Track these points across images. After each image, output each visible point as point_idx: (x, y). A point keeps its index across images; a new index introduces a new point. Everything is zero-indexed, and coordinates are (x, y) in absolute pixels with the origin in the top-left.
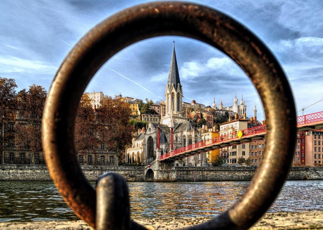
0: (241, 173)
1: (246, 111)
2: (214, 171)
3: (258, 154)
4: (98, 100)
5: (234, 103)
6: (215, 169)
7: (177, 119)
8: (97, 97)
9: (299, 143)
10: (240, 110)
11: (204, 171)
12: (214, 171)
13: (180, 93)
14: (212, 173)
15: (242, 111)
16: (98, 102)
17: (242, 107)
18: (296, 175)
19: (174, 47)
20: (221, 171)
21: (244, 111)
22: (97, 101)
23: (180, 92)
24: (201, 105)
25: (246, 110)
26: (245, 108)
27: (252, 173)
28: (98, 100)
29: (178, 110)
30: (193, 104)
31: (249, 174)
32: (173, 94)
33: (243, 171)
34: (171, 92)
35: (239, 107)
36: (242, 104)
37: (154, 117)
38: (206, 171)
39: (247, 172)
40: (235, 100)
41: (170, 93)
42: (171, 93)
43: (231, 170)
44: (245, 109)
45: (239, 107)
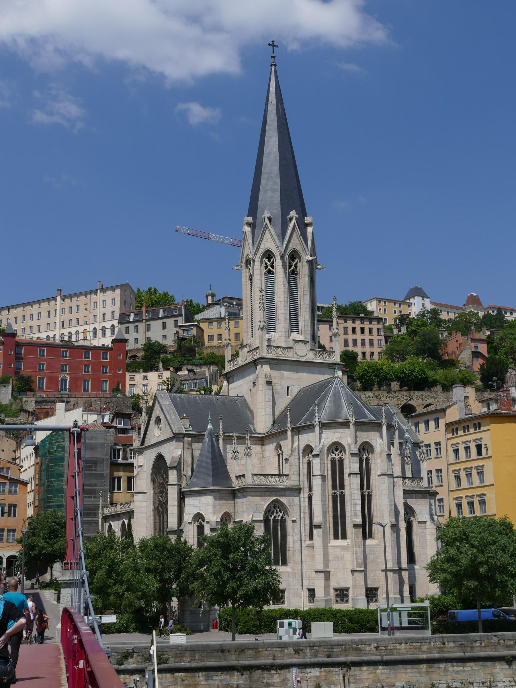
4: (113, 312)
8: (109, 302)
11: (359, 664)
13: (302, 253)
16: (113, 319)
22: (108, 316)
23: (299, 248)
28: (113, 312)
34: (258, 248)
41: (255, 254)
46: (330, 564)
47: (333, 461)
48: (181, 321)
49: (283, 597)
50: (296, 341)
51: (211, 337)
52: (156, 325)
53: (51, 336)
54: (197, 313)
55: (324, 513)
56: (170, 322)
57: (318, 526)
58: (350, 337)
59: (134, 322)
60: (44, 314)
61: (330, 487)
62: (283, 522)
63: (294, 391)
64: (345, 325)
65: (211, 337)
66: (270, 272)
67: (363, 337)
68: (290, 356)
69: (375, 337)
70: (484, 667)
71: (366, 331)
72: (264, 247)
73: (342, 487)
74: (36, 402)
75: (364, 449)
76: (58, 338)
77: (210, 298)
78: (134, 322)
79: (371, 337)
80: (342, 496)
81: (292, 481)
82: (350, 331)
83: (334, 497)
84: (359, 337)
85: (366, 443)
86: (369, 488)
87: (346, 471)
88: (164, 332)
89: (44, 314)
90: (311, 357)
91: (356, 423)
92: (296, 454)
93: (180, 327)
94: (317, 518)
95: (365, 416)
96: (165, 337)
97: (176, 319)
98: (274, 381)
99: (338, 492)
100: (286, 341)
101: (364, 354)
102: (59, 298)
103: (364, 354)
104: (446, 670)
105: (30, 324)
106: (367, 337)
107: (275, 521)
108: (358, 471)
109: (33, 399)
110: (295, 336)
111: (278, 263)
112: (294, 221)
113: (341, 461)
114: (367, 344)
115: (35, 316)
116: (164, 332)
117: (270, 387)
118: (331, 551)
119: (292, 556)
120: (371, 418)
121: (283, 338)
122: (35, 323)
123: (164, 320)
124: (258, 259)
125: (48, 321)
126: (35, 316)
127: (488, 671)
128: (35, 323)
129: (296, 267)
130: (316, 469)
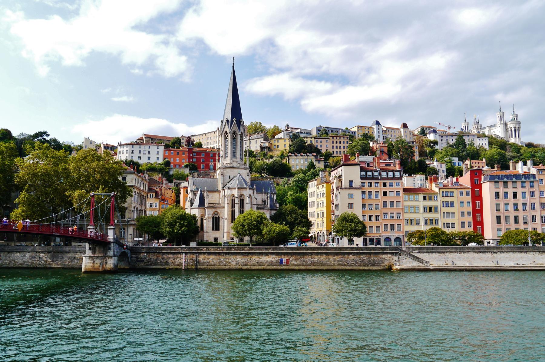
1: (521, 132)
3: (381, 218)
5: (498, 119)
7: (229, 170)
9: (469, 196)
10: (509, 129)
13: (237, 132)
14: (212, 257)
15: (513, 131)
17: (511, 126)
18: (370, 261)
20: (228, 253)
21: (517, 131)
23: (236, 130)
24: (425, 129)
25: (521, 129)
26: (517, 126)
29: (234, 155)
30: (402, 130)
31: (277, 259)
32: (227, 134)
34: (223, 130)
35: (506, 125)
36: (512, 120)
37: (306, 157)
39: (275, 256)
40: (498, 114)
41: (222, 132)
42: (224, 131)
44: (519, 127)
45: (506, 125)
47: (232, 200)
48: (262, 140)
49: (217, 240)
50: (233, 161)
53: (215, 146)
54: (276, 135)
55: (228, 215)
56: (258, 140)
58: (335, 145)
60: (212, 137)
61: (231, 208)
62: (219, 218)
63: (231, 177)
64: (333, 140)
66: (227, 138)
67: (340, 145)
68: (231, 165)
69: (346, 145)
71: (342, 142)
73: (234, 208)
74: (198, 174)
75: (242, 196)
76: (217, 147)
77: (287, 127)
79: (344, 145)
80: (234, 210)
81: (222, 205)
82: (335, 142)
83: (232, 210)
84: (338, 145)
85: (242, 194)
86: (243, 208)
87: (236, 203)
89: (212, 137)
90: (238, 166)
91: (238, 188)
92: (223, 197)
93: (262, 142)
94: (226, 217)
98: (225, 174)
99: (233, 209)
100: (230, 161)
101: (337, 152)
102: (218, 131)
103: (337, 152)
104: (223, 255)
105: (208, 141)
106: (342, 145)
107: (216, 217)
109: (196, 173)
110: (234, 159)
111: (229, 135)
113: (234, 200)
114: (338, 148)
115: (209, 138)
116: (256, 145)
117: (223, 176)
119: (221, 228)
120: (245, 186)
121: (229, 160)
122: (209, 141)
123: (256, 140)
124: (223, 134)
125: (214, 140)
126: (209, 138)
128: (209, 141)
129: (235, 136)
130: (226, 202)
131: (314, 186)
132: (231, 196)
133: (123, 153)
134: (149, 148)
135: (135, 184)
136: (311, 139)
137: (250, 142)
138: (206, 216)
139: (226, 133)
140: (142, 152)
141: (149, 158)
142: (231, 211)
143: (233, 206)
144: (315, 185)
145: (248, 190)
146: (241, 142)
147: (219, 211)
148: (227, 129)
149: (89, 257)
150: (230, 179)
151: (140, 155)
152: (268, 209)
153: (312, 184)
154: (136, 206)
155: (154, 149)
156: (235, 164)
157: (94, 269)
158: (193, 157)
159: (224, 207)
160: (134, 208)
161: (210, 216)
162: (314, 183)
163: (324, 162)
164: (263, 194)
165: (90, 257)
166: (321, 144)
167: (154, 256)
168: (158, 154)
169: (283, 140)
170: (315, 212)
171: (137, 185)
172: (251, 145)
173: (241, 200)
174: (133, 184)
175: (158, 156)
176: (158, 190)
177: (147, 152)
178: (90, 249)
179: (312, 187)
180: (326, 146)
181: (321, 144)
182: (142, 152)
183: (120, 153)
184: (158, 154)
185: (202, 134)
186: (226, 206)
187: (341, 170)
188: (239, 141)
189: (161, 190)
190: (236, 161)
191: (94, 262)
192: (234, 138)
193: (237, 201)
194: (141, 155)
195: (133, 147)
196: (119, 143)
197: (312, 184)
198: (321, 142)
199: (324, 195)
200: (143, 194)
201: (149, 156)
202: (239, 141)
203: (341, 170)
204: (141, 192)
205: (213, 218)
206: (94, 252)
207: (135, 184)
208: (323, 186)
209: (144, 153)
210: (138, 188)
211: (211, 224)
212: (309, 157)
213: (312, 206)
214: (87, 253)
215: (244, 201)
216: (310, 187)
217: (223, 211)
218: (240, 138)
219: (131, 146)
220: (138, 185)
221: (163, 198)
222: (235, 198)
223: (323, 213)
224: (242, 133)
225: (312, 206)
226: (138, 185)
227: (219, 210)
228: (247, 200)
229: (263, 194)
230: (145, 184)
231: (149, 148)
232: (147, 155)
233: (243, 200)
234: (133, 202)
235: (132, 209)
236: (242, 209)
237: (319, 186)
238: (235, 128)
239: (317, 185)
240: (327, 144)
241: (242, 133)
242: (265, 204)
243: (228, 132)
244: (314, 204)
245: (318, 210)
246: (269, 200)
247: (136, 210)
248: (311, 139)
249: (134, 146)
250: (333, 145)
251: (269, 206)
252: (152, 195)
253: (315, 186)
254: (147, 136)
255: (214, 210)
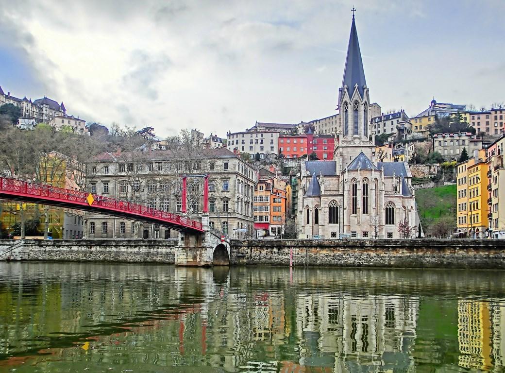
0: (389, 251)
2: (331, 247)
6: (333, 242)
7: (349, 150)
12: (331, 247)
13: (360, 101)
14: (324, 252)
19: (354, 16)
23: (358, 99)
27: (417, 253)
29: (356, 131)
32: (347, 104)
33: (394, 248)
37: (458, 138)
38: (314, 247)
39: (405, 251)
42: (343, 102)
43: (367, 247)
46: (351, 223)
47: (353, 185)
50: (355, 138)
51: (416, 127)
52: (388, 123)
55: (348, 204)
56: (395, 121)
57: (345, 209)
59: (378, 122)
61: (352, 195)
63: (353, 159)
64: (496, 115)
65: (416, 127)
66: (347, 111)
70: (352, 249)
72: (344, 100)
73: (356, 195)
78: (378, 122)
80: (356, 198)
82: (498, 118)
83: (353, 198)
88: (392, 126)
90: (362, 144)
92: (342, 182)
94: (346, 205)
95: (366, 167)
96: (392, 129)
97: (398, 119)
99: (355, 197)
105: (332, 127)
107: (334, 207)
108: (362, 189)
112: (356, 88)
113: (356, 185)
115: (334, 123)
116: (392, 126)
118: (351, 218)
123: (392, 120)
124: (342, 105)
126: (334, 123)
127: (353, 250)
131: (465, 170)
132: (352, 180)
133: (233, 144)
134: (262, 136)
135: (239, 170)
136: (465, 115)
137: (385, 124)
138: (322, 206)
139: (346, 103)
140: (254, 141)
141: (262, 148)
142: (352, 199)
143: (355, 193)
144: (467, 168)
145: (373, 171)
146: (365, 115)
147: (337, 200)
148: (346, 98)
149: (181, 249)
150: (352, 161)
151: (251, 145)
152: (400, 197)
153: (462, 167)
154: (241, 196)
155: (267, 137)
156: (357, 142)
157: (188, 261)
158: (313, 146)
159: (343, 195)
160: (238, 199)
161: (327, 206)
162: (465, 166)
163: (483, 144)
164: (394, 179)
165: (183, 248)
166: (479, 121)
167: (257, 250)
168: (272, 143)
169: (427, 119)
170: (467, 204)
171: (240, 172)
172: (385, 128)
173: (364, 185)
174: (237, 170)
175: (272, 146)
176: (269, 182)
177: (259, 141)
178: (182, 239)
179: (462, 171)
180: (485, 123)
181: (479, 121)
182: (254, 141)
183: (229, 144)
184: (272, 143)
185: (325, 119)
186: (346, 193)
187: (502, 144)
188: (362, 113)
189: (273, 181)
190: (359, 138)
191: (187, 254)
192: (356, 109)
193: (360, 187)
194: (253, 145)
195: (243, 137)
196: (227, 133)
197: (462, 167)
198: (479, 118)
199: (478, 180)
200: (249, 183)
201: (262, 145)
202: (362, 113)
203: (502, 144)
204: (246, 181)
205: (330, 208)
206: (186, 244)
207: (239, 170)
208: (477, 169)
209: (257, 143)
210: (241, 176)
211: (327, 215)
212: (461, 138)
213: (463, 196)
214: (179, 244)
215: (368, 186)
216: (459, 172)
217: (342, 200)
218: (363, 110)
219: (242, 135)
220: (242, 172)
221: (275, 191)
222: (357, 183)
223: (477, 204)
224: (366, 102)
225: (463, 196)
226: (242, 172)
227: (337, 199)
228: (371, 186)
229: (394, 179)
230: (251, 172)
231: (262, 136)
232: (259, 145)
233: (367, 185)
234: (236, 192)
235: (236, 200)
236: (365, 196)
237: (472, 169)
238: (356, 97)
239: (469, 168)
240: (488, 120)
241: (366, 102)
242: (396, 190)
243: (348, 101)
244: (465, 193)
245: (471, 200)
246: (401, 185)
247: (240, 200)
248: (465, 115)
249: (245, 135)
250: (496, 121)
251: (401, 193)
252: (262, 187)
253: (467, 170)
254: (261, 125)
255: (331, 199)
